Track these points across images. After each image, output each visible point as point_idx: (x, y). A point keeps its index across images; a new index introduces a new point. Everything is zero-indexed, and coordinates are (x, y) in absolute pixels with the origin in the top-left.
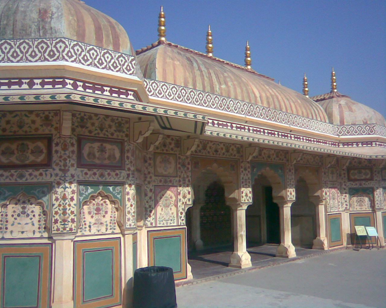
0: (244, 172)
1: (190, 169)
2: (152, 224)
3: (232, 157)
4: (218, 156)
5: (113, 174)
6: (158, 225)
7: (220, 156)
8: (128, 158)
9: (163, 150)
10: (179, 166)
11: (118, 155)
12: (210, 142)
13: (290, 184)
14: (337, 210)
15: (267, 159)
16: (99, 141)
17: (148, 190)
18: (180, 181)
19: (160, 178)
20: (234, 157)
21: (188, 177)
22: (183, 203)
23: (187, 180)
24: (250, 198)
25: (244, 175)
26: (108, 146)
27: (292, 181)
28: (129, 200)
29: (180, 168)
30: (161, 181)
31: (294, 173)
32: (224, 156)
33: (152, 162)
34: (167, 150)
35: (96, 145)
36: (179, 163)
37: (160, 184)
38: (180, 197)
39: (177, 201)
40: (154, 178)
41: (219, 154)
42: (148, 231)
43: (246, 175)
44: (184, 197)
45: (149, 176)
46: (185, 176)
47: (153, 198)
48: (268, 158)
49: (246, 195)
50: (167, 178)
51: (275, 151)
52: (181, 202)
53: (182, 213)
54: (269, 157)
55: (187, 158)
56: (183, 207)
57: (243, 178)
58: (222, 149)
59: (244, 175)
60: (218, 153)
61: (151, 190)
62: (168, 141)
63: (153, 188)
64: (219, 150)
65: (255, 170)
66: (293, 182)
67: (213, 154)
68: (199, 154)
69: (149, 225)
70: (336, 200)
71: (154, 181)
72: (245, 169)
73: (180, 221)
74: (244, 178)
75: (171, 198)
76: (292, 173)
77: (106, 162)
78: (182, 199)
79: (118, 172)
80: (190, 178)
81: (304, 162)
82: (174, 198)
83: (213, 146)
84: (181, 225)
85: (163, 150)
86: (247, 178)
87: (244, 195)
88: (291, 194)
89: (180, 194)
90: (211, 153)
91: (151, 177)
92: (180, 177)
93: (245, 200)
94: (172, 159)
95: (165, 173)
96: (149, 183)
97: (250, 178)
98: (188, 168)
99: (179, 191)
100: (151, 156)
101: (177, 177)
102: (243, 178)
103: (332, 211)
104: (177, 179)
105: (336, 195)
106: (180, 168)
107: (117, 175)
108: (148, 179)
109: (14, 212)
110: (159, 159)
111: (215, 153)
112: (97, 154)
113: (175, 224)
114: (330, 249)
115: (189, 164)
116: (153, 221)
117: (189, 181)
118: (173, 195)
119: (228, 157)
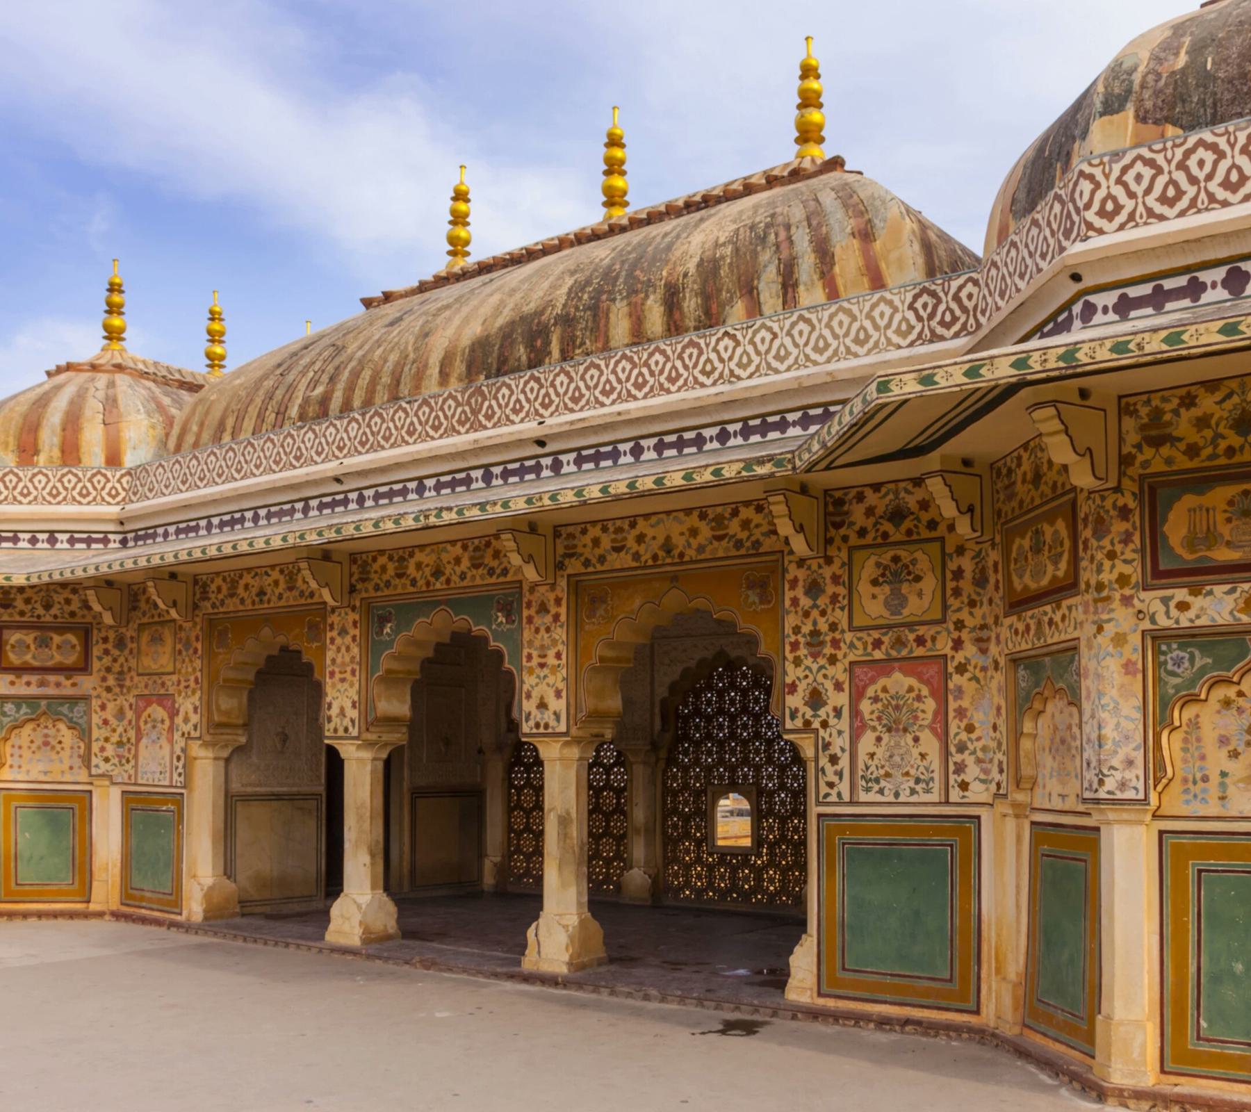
0: (338, 641)
2: (130, 777)
3: (303, 601)
4: (266, 606)
6: (140, 781)
7: (272, 605)
9: (153, 616)
10: (179, 646)
12: (245, 573)
13: (542, 666)
14: (934, 797)
15: (428, 584)
18: (179, 683)
19: (146, 678)
20: (309, 601)
21: (194, 669)
22: (183, 734)
23: (192, 678)
24: (353, 721)
25: (339, 650)
27: (551, 653)
29: (180, 652)
30: (146, 686)
31: (563, 618)
32: (282, 603)
33: (135, 645)
38: (179, 720)
39: (171, 729)
40: (136, 679)
41: (269, 601)
43: (343, 649)
44: (186, 720)
45: (128, 677)
46: (190, 670)
48: (432, 580)
49: (342, 713)
50: (156, 677)
51: (465, 548)
52: (180, 733)
53: (179, 758)
54: (437, 573)
56: (183, 744)
57: (334, 661)
58: (276, 583)
59: (339, 650)
60: (266, 598)
63: (132, 700)
64: (269, 590)
65: (387, 630)
66: (558, 656)
67: (253, 603)
68: (221, 610)
69: (126, 776)
72: (343, 632)
73: (175, 776)
74: (339, 661)
76: (556, 618)
78: (182, 725)
81: (636, 556)
82: (167, 723)
83: (252, 582)
86: (347, 659)
87: (334, 711)
88: (542, 705)
90: (248, 601)
91: (132, 678)
92: (180, 672)
93: (336, 730)
94: (168, 635)
96: (129, 690)
97: (358, 659)
101: (173, 673)
102: (334, 661)
103: (863, 797)
104: (175, 678)
105: (930, 705)
108: (128, 683)
109: (32, 742)
110: (145, 637)
111: (257, 599)
114: (821, 1002)
115: (197, 639)
116: (132, 772)
119: (292, 602)
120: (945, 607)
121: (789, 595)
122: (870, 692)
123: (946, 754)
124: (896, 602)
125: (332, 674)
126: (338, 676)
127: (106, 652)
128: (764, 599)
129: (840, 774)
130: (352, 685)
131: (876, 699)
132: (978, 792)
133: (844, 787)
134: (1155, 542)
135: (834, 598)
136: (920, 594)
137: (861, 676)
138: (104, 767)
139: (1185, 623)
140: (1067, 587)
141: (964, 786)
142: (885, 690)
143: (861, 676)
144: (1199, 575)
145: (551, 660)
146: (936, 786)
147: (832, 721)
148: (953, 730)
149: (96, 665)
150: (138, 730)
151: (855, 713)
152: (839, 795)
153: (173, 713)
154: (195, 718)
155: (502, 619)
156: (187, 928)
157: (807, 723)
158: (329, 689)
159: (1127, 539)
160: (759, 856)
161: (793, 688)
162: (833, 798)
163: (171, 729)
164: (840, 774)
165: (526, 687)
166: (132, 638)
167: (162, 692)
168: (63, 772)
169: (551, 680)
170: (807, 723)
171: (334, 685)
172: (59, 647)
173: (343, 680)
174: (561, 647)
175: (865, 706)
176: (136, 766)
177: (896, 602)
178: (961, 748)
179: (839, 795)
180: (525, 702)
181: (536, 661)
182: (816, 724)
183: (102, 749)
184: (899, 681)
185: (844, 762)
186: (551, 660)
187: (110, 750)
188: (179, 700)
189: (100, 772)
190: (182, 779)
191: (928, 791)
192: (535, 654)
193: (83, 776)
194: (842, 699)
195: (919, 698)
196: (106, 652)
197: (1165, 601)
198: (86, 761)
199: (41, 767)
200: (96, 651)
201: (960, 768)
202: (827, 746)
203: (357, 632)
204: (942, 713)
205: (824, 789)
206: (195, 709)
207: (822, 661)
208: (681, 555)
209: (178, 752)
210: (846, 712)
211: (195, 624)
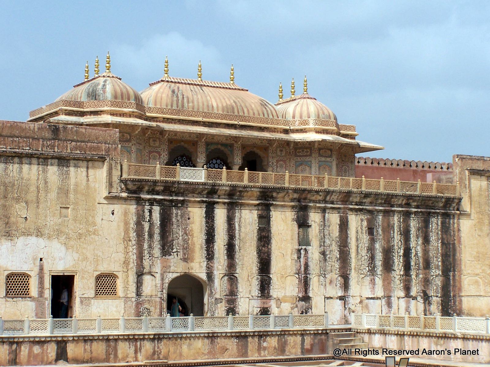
5: (127, 144)
11: (129, 137)
26: (125, 134)
44: (164, 156)
62: (157, 132)
77: (124, 140)
82: (158, 157)
94: (158, 140)
105: (284, 166)
108: (146, 148)
110: (151, 140)
134: (319, 153)
137: (277, 161)
143: (277, 161)
144: (322, 156)
145: (239, 155)
153: (160, 155)
154: (166, 156)
163: (160, 158)
175: (278, 165)
184: (281, 162)
186: (239, 155)
194: (276, 164)
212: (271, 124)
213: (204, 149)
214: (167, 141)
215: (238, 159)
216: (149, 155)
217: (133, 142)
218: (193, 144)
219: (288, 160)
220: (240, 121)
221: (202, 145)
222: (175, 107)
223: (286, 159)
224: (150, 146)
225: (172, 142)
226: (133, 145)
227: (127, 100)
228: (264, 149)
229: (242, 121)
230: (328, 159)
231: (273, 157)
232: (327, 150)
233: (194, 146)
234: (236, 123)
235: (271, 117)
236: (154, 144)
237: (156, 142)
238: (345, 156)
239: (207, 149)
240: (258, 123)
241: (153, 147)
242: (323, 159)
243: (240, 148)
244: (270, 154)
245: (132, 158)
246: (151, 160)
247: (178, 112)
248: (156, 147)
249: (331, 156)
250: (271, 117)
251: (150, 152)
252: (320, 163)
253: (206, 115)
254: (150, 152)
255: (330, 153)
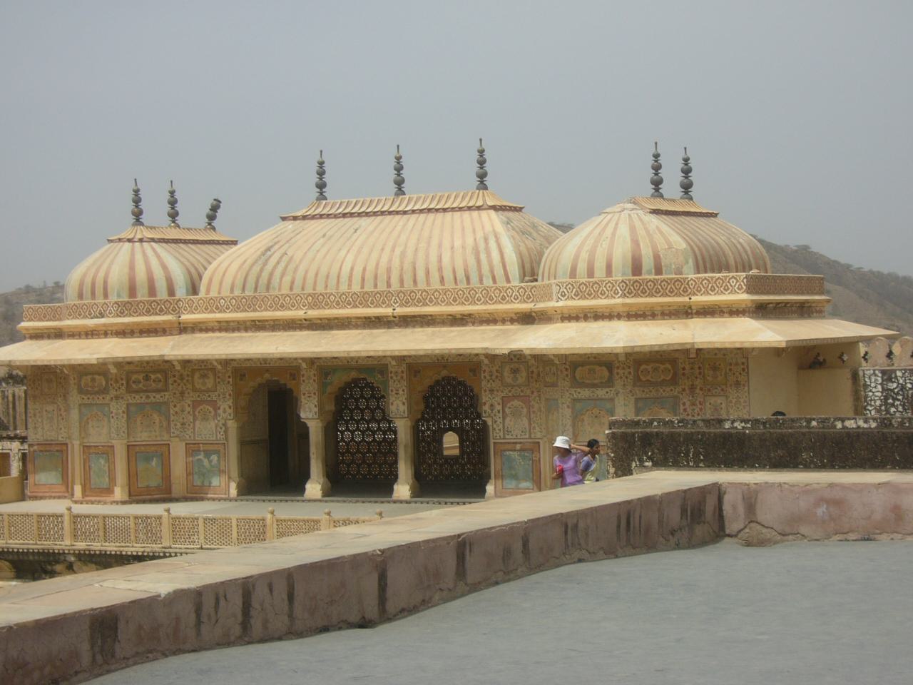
1: (231, 383)
2: (190, 437)
6: (197, 438)
8: (111, 385)
9: (201, 366)
10: (218, 380)
11: (104, 383)
13: (397, 394)
16: (90, 374)
17: (186, 405)
18: (219, 395)
19: (198, 393)
23: (227, 394)
26: (97, 377)
28: (113, 417)
29: (219, 382)
30: (199, 396)
31: (405, 377)
33: (190, 378)
34: (205, 366)
35: (89, 377)
36: (219, 377)
37: (199, 399)
38: (220, 411)
39: (216, 414)
41: (270, 364)
42: (186, 444)
44: (225, 412)
47: (191, 413)
53: (221, 428)
55: (228, 371)
56: (223, 422)
61: (189, 405)
66: (403, 391)
67: (261, 364)
69: (188, 437)
70: (525, 418)
71: (193, 397)
73: (219, 436)
75: (210, 412)
76: (402, 377)
77: (96, 389)
79: (104, 396)
80: (231, 392)
84: (220, 440)
85: (201, 366)
89: (219, 408)
95: (203, 388)
98: (229, 382)
99: (218, 405)
100: (189, 373)
103: (507, 437)
105: (525, 410)
106: (219, 382)
107: (103, 398)
108: (186, 395)
110: (197, 375)
112: (90, 384)
113: (214, 439)
115: (229, 377)
117: (230, 395)
118: (211, 409)
120: (529, 382)
121: (483, 375)
122: (508, 405)
123: (530, 424)
124: (515, 379)
125: (304, 394)
126: (307, 395)
127: (175, 381)
128: (475, 375)
129: (500, 430)
130: (314, 398)
131: (510, 408)
132: (539, 435)
133: (501, 434)
135: (497, 377)
136: (522, 377)
137: (504, 401)
138: (177, 433)
139: (579, 397)
140: (554, 385)
141: (535, 433)
142: (512, 405)
143: (504, 401)
146: (527, 434)
147: (497, 414)
148: (532, 417)
149: (171, 387)
150: (194, 416)
151: (504, 412)
152: (500, 436)
153: (216, 408)
154: (229, 411)
155: (379, 376)
156: (231, 500)
157: (489, 415)
158: (303, 400)
159: (567, 375)
160: (463, 459)
161: (485, 404)
162: (498, 437)
163: (216, 414)
164: (500, 430)
165: (391, 401)
166: (188, 375)
167: (209, 399)
168: (156, 437)
169: (401, 399)
170: (489, 415)
171: (305, 399)
172: (154, 381)
173: (309, 397)
174: (404, 388)
176: (194, 434)
177: (515, 379)
178: (534, 422)
179: (500, 436)
180: (391, 407)
181: (393, 393)
182: (492, 415)
183: (175, 425)
184: (516, 403)
185: (501, 426)
186: (401, 392)
187: (179, 425)
188: (219, 403)
189: (175, 435)
190: (224, 437)
191: (525, 435)
192: (394, 390)
193: (166, 437)
194: (500, 408)
195: (522, 408)
196: (175, 381)
197: (575, 391)
198: (169, 432)
199: (146, 434)
200: (171, 381)
201: (534, 428)
202: (496, 422)
203: (316, 378)
204: (529, 412)
205: (495, 435)
206: (230, 407)
207: (494, 396)
208: (447, 360)
209: (221, 425)
210: (501, 411)
211: (228, 371)
212: (485, 303)
213: (316, 386)
214: (230, 374)
215: (401, 404)
216: (193, 412)
217: (113, 393)
218: (291, 374)
219: (536, 394)
220: (401, 305)
221: (309, 378)
222: (249, 293)
223: (528, 392)
224: (194, 390)
225: (244, 375)
226: (112, 398)
227: (102, 297)
228: (471, 370)
229: (407, 304)
230: (601, 393)
231: (492, 391)
232: (597, 368)
233: (294, 379)
234: (389, 311)
235: (488, 282)
236: (204, 384)
237: (206, 380)
238: (715, 368)
239: (323, 386)
240: (449, 304)
241: (201, 391)
242: (585, 393)
243: (404, 375)
244: (484, 383)
245: (113, 429)
246: (197, 423)
247: (251, 304)
248: (208, 391)
249: (609, 383)
250: (488, 282)
251: (195, 404)
252: (578, 406)
253: (317, 300)
254: (195, 404)
255: (606, 373)
